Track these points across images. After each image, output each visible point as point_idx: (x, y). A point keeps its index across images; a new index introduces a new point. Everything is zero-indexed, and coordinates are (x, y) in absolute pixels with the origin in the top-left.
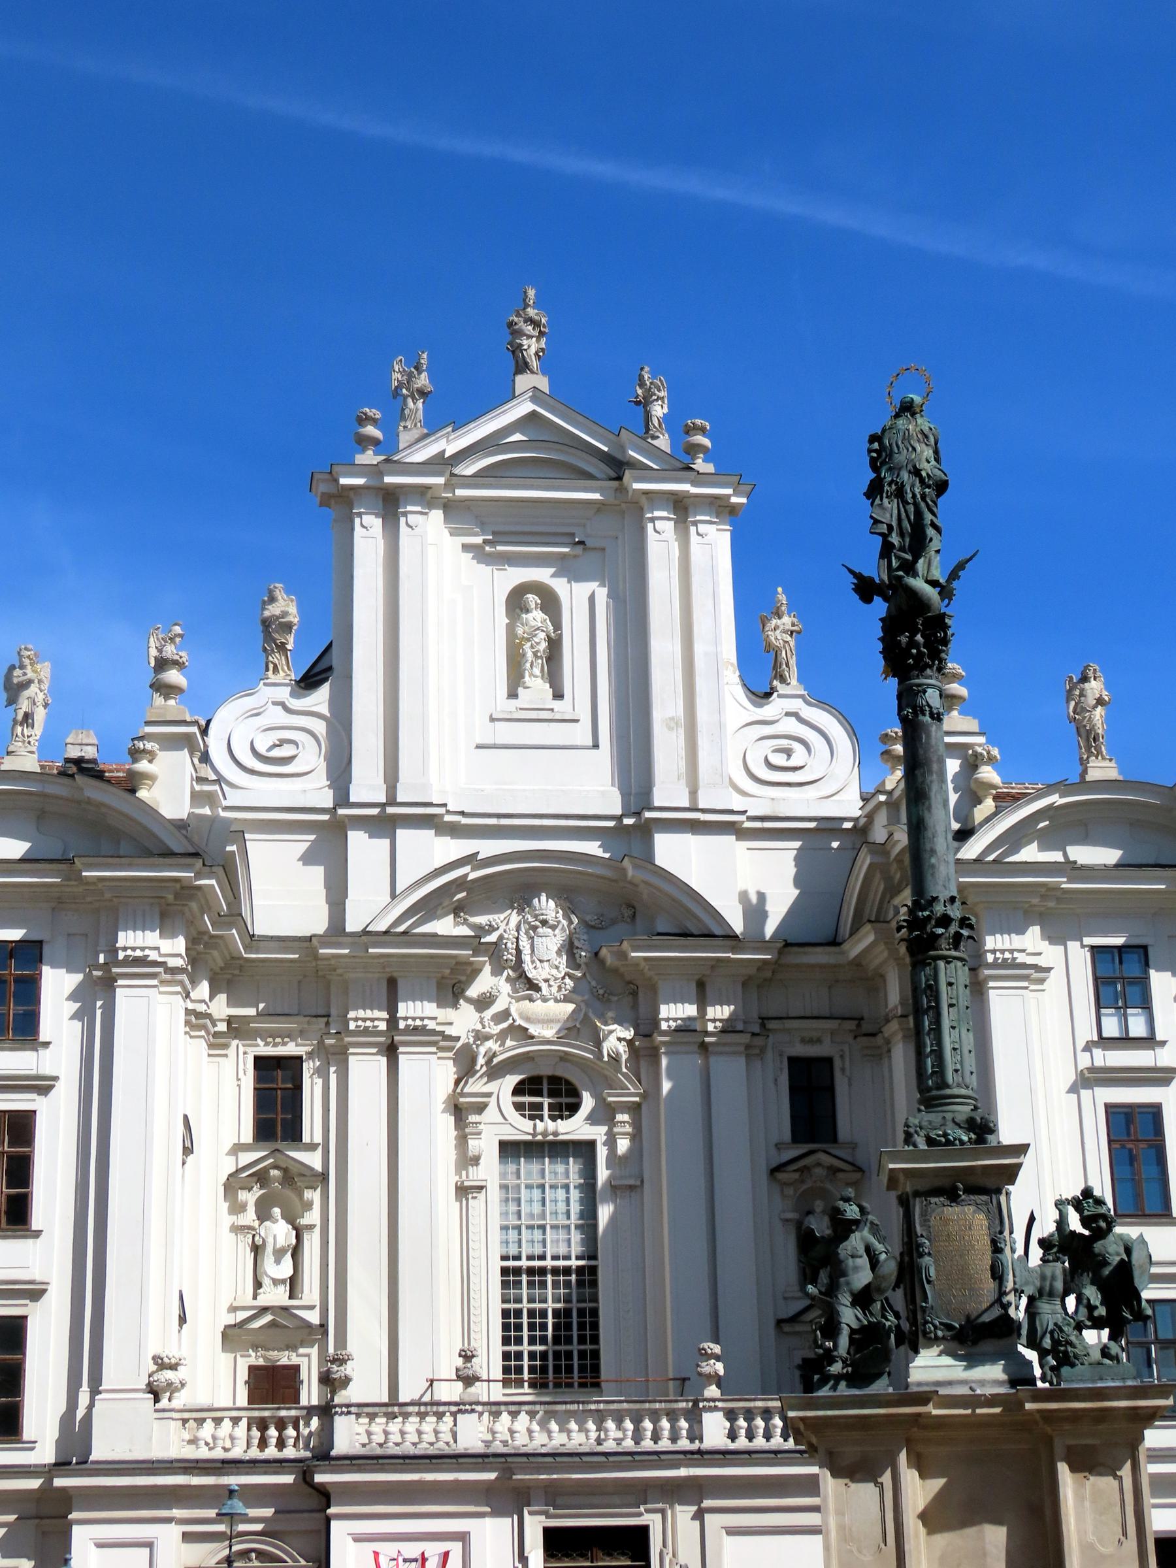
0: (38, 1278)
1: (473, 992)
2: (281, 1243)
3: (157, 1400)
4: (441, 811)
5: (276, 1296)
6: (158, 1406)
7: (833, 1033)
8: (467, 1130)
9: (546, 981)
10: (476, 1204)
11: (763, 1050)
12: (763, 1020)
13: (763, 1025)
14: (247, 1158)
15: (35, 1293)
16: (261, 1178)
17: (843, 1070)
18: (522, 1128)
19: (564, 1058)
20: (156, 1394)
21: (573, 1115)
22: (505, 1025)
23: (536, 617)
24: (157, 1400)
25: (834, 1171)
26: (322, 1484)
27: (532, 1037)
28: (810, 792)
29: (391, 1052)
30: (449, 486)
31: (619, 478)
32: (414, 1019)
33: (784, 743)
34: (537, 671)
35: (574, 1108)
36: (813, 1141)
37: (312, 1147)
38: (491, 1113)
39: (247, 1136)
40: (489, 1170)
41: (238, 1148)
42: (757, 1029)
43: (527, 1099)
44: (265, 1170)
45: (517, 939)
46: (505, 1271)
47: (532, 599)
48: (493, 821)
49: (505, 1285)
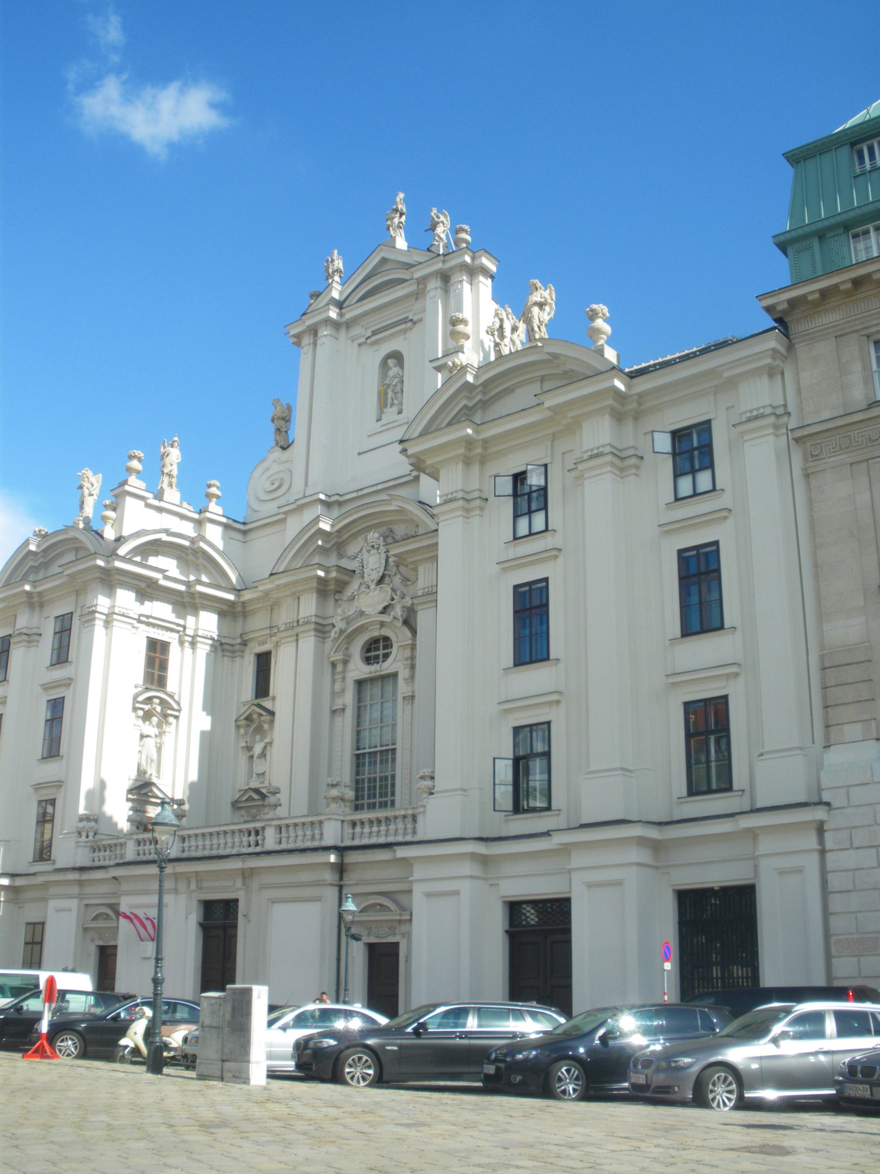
9: (372, 581)
19: (382, 624)
23: (394, 371)
35: (391, 653)
38: (351, 666)
40: (349, 698)
47: (391, 362)
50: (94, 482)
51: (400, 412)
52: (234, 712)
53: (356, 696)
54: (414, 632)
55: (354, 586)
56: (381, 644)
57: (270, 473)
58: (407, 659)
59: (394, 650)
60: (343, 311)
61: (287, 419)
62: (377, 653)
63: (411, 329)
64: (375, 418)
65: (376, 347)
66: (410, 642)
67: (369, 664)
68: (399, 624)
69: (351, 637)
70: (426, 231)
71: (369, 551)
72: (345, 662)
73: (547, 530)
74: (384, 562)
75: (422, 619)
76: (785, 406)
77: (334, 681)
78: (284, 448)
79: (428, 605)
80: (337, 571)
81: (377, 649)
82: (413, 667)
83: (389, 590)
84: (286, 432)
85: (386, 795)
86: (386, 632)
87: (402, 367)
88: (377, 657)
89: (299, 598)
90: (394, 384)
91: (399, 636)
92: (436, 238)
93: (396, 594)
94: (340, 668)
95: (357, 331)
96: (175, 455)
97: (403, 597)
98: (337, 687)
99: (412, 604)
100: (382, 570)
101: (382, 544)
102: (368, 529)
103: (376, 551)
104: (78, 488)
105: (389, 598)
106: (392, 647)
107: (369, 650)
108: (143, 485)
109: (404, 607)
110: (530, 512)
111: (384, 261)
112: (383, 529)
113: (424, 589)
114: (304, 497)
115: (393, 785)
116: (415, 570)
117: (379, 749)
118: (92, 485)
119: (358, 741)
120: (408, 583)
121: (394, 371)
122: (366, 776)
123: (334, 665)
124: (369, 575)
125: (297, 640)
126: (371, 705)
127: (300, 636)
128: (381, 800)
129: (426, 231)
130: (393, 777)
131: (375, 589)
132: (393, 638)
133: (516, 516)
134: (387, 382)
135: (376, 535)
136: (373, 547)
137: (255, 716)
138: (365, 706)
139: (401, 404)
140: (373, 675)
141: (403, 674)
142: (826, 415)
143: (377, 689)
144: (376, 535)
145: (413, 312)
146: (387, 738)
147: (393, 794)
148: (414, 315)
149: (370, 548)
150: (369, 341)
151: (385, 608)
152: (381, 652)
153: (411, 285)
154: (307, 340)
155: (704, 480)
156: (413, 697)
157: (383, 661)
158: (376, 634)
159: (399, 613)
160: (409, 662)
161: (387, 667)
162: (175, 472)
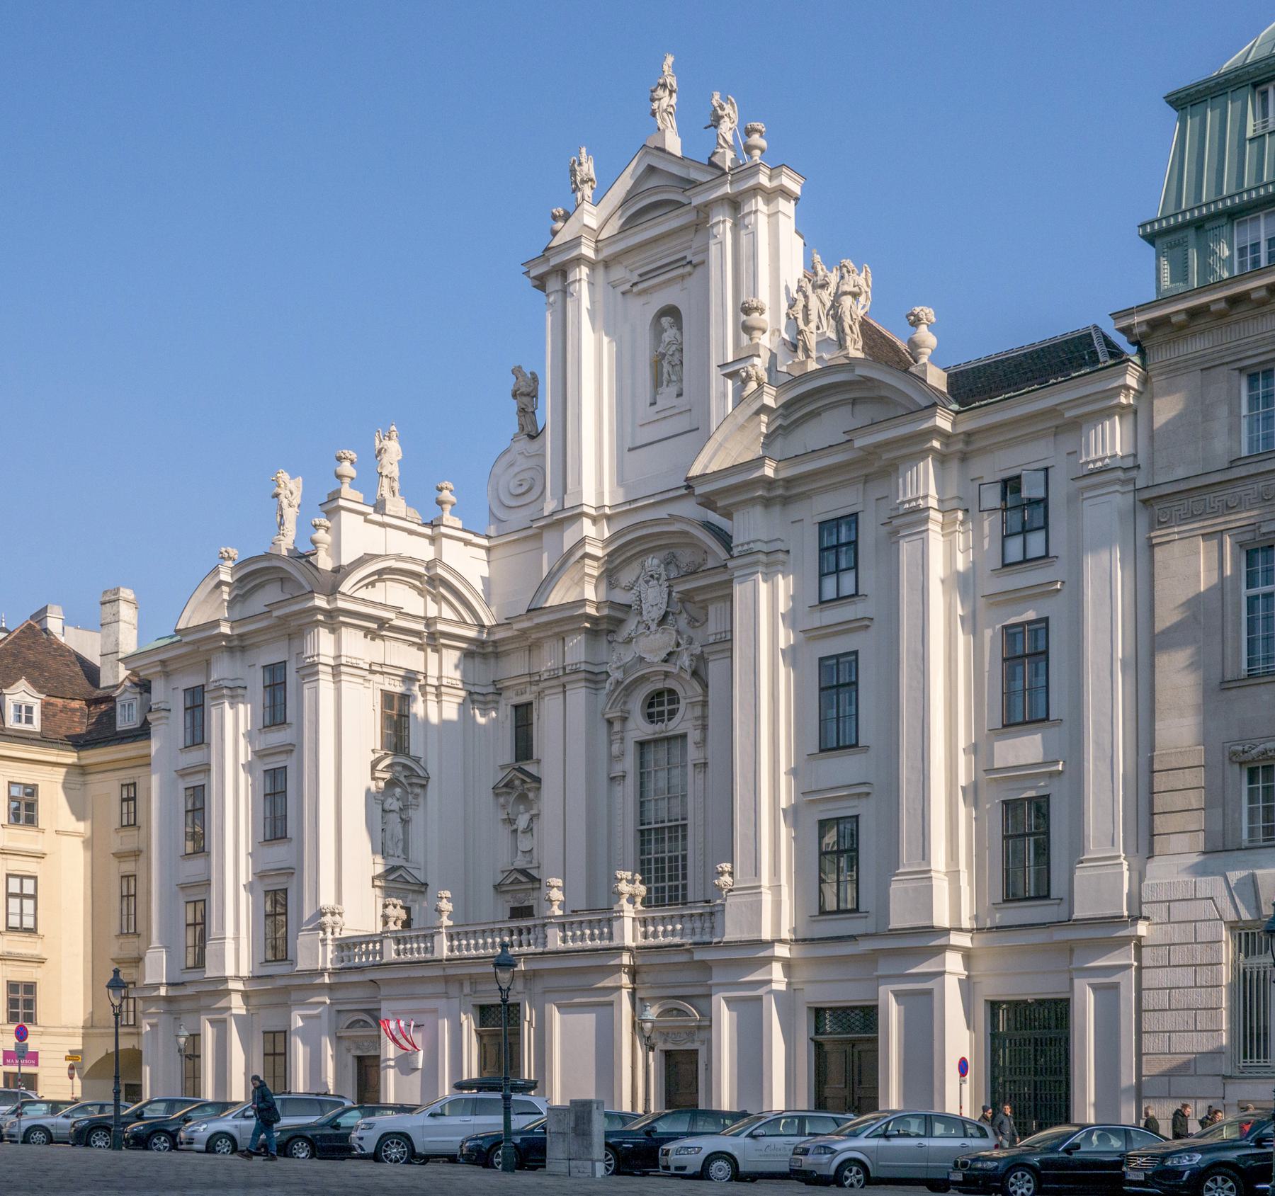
9: (653, 620)
10: (618, 789)
19: (667, 675)
21: (672, 718)
29: (564, 686)
35: (678, 709)
38: (631, 724)
40: (629, 764)
41: (503, 767)
44: (511, 781)
50: (292, 488)
51: (680, 395)
53: (638, 762)
54: (705, 686)
56: (666, 698)
57: (516, 469)
58: (697, 718)
59: (682, 705)
61: (532, 395)
62: (661, 709)
66: (701, 698)
67: (653, 722)
68: (687, 676)
69: (630, 689)
70: (706, 128)
71: (647, 582)
72: (624, 719)
73: (857, 594)
74: (666, 596)
75: (714, 670)
77: (611, 743)
78: (532, 437)
79: (721, 655)
80: (609, 607)
81: (662, 704)
82: (704, 728)
83: (674, 633)
84: (533, 413)
85: (677, 879)
86: (670, 684)
87: (680, 329)
88: (661, 714)
89: (564, 639)
90: (671, 353)
91: (688, 691)
92: (721, 142)
93: (682, 638)
94: (617, 727)
96: (394, 449)
97: (690, 641)
98: (616, 748)
99: (702, 652)
100: (664, 607)
101: (664, 573)
102: (645, 552)
103: (656, 582)
104: (273, 497)
105: (673, 642)
106: (678, 703)
107: (651, 705)
108: (359, 496)
109: (692, 655)
110: (838, 571)
112: (664, 553)
113: (716, 634)
114: (563, 509)
115: (684, 867)
116: (705, 608)
117: (667, 824)
118: (292, 493)
119: (642, 813)
120: (697, 624)
121: (669, 335)
122: (653, 856)
123: (610, 722)
124: (649, 612)
125: (564, 692)
126: (656, 771)
127: (568, 687)
128: (671, 883)
129: (706, 128)
130: (684, 858)
131: (657, 631)
132: (681, 694)
133: (822, 575)
134: (661, 350)
135: (656, 561)
136: (652, 576)
138: (649, 773)
139: (681, 380)
140: (657, 736)
141: (694, 736)
143: (662, 752)
144: (656, 561)
146: (677, 811)
147: (685, 877)
149: (648, 578)
151: (670, 654)
152: (666, 708)
156: (705, 764)
157: (669, 720)
158: (659, 686)
159: (687, 663)
160: (700, 722)
161: (674, 727)
162: (396, 473)
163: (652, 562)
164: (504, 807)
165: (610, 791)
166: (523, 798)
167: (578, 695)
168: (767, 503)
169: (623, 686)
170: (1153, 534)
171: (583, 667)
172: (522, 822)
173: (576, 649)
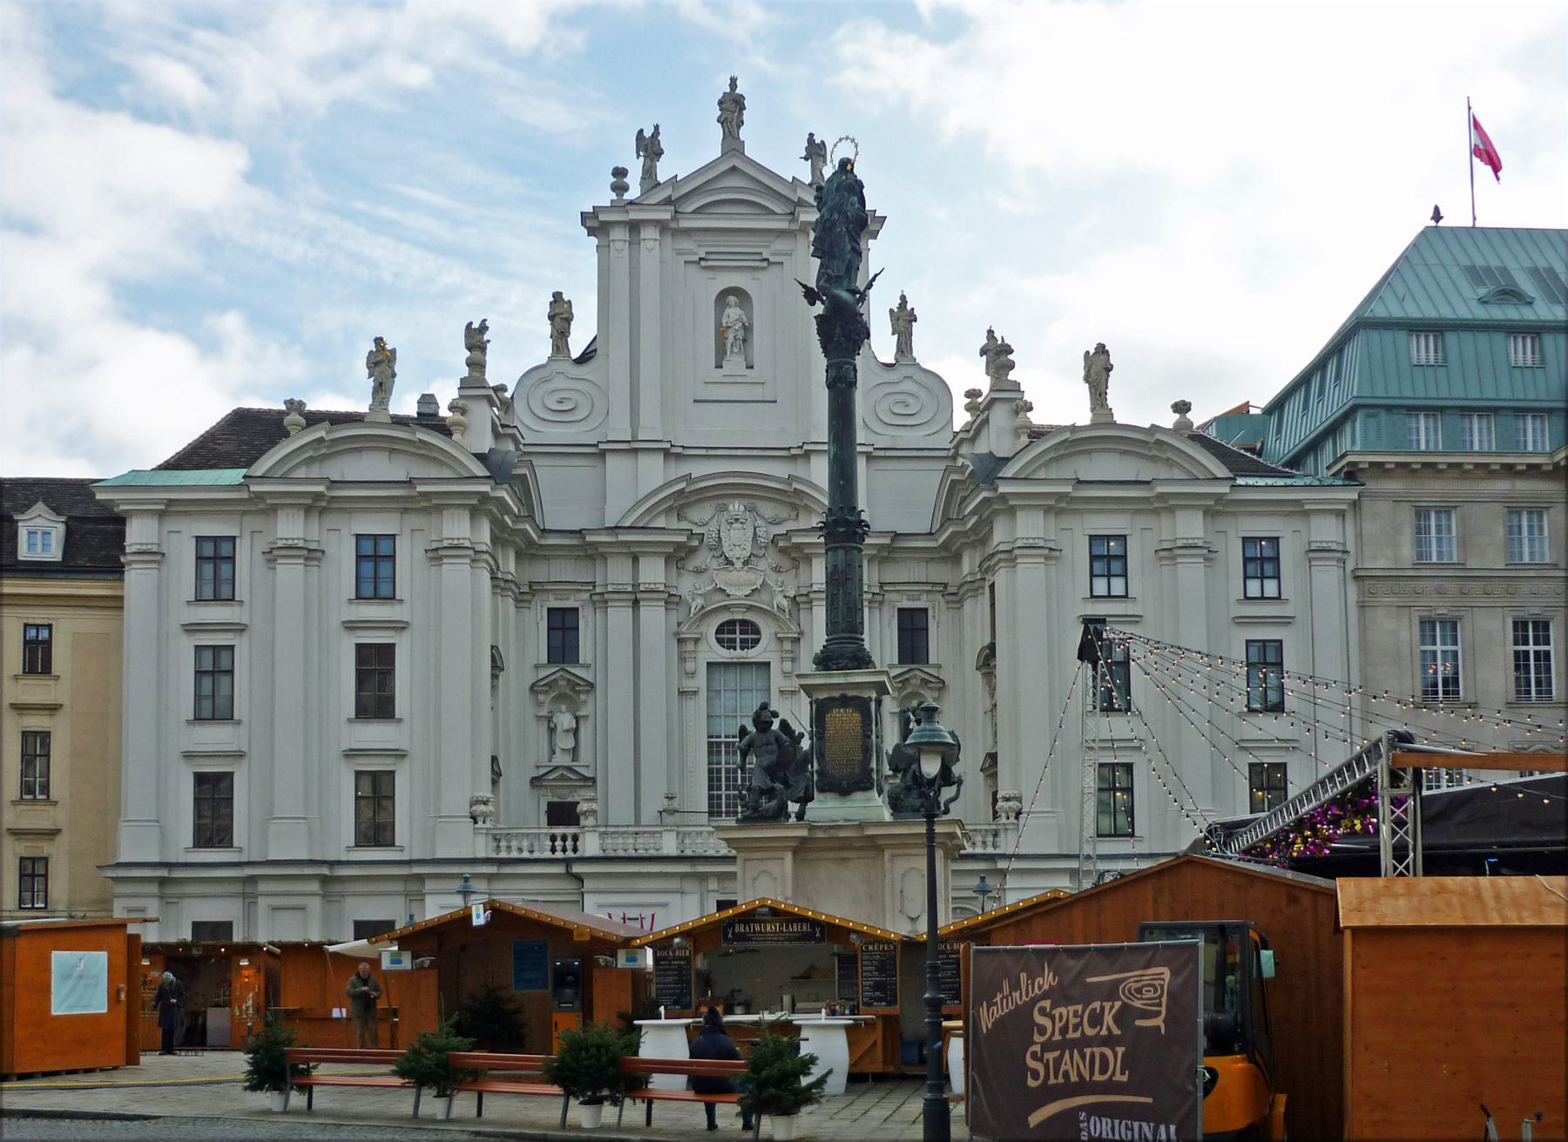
0: (402, 748)
1: (691, 565)
2: (566, 727)
3: (476, 822)
4: (668, 445)
5: (562, 759)
6: (476, 826)
7: (928, 592)
8: (687, 655)
9: (738, 558)
10: (690, 703)
11: (881, 603)
12: (882, 584)
13: (881, 587)
14: (543, 673)
15: (400, 755)
16: (551, 685)
17: (934, 617)
18: (724, 655)
19: (750, 608)
20: (474, 819)
22: (710, 588)
23: (733, 313)
24: (476, 822)
25: (925, 682)
26: (577, 873)
27: (729, 595)
28: (921, 432)
29: (636, 603)
30: (674, 219)
31: (792, 214)
32: (650, 584)
33: (902, 397)
34: (735, 350)
35: (757, 641)
36: (913, 663)
37: (587, 666)
38: (702, 646)
39: (544, 659)
40: (701, 681)
42: (877, 590)
43: (726, 636)
45: (719, 531)
46: (710, 745)
48: (703, 452)
49: (710, 753)
52: (518, 676)
55: (703, 558)
57: (552, 386)
60: (679, 216)
63: (763, 268)
64: (713, 363)
65: (709, 274)
69: (705, 615)
72: (697, 640)
76: (1344, 544)
94: (690, 646)
95: (687, 244)
98: (690, 666)
111: (734, 169)
112: (746, 502)
136: (737, 520)
137: (562, 683)
140: (735, 660)
142: (1381, 564)
143: (731, 678)
145: (772, 250)
148: (772, 254)
150: (703, 263)
152: (738, 636)
153: (783, 220)
154: (619, 234)
155: (1271, 588)
158: (740, 617)
163: (736, 507)
164: (540, 704)
165: (680, 703)
166: (561, 698)
167: (654, 616)
168: (1048, 510)
169: (704, 611)
170: (1367, 599)
171: (662, 588)
172: (565, 720)
173: (653, 572)
